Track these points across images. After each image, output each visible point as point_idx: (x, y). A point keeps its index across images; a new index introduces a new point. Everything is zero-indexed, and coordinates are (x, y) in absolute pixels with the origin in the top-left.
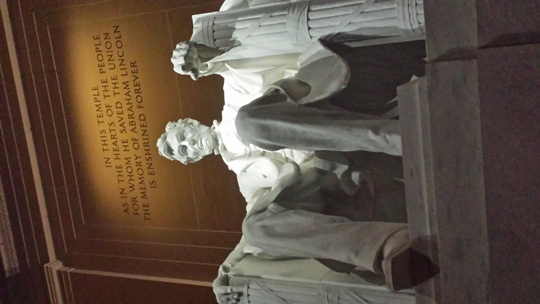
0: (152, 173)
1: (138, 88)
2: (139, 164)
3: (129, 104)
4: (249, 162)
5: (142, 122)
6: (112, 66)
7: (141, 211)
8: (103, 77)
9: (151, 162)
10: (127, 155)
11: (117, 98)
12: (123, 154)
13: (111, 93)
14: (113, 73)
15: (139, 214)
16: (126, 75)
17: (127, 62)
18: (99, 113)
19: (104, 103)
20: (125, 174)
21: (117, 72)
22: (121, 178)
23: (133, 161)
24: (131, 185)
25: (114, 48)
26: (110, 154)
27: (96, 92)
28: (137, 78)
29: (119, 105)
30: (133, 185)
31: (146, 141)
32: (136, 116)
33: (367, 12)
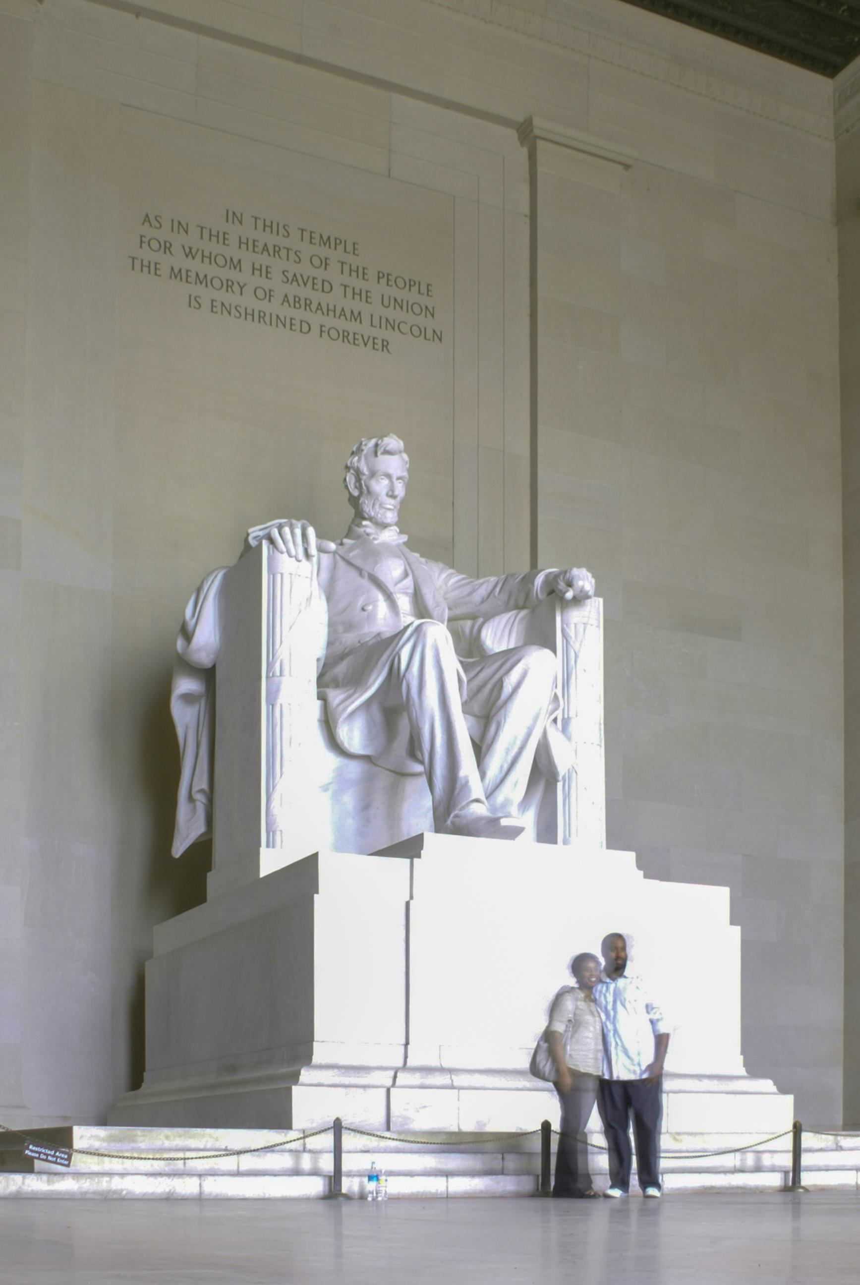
0: (214, 309)
1: (351, 338)
2: (228, 285)
3: (328, 310)
6: (386, 302)
7: (146, 254)
8: (372, 274)
9: (232, 314)
10: (246, 266)
11: (338, 290)
12: (248, 258)
15: (141, 247)
16: (372, 325)
20: (213, 247)
23: (234, 275)
24: (194, 251)
28: (366, 345)
29: (327, 287)
30: (193, 258)
31: (267, 319)
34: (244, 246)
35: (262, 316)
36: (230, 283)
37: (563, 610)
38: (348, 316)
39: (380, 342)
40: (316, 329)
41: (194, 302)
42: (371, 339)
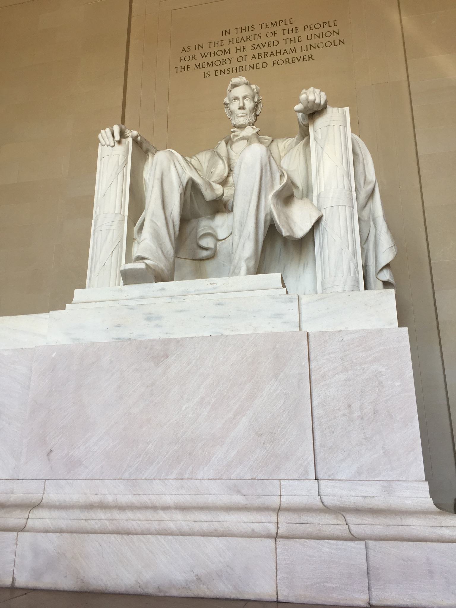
2: (224, 62)
4: (224, 158)
5: (261, 65)
6: (310, 38)
7: (184, 64)
10: (233, 51)
11: (282, 42)
12: (232, 47)
13: (287, 36)
14: (303, 37)
17: (313, 52)
18: (270, 24)
19: (279, 29)
20: (216, 49)
21: (305, 42)
22: (212, 44)
24: (206, 54)
25: (325, 40)
26: (233, 35)
27: (288, 22)
29: (276, 43)
31: (244, 69)
32: (267, 60)
33: (341, 253)
34: (231, 43)
35: (241, 69)
36: (224, 60)
37: (313, 123)
38: (288, 52)
39: (307, 57)
40: (270, 64)
41: (207, 75)
42: (302, 57)
